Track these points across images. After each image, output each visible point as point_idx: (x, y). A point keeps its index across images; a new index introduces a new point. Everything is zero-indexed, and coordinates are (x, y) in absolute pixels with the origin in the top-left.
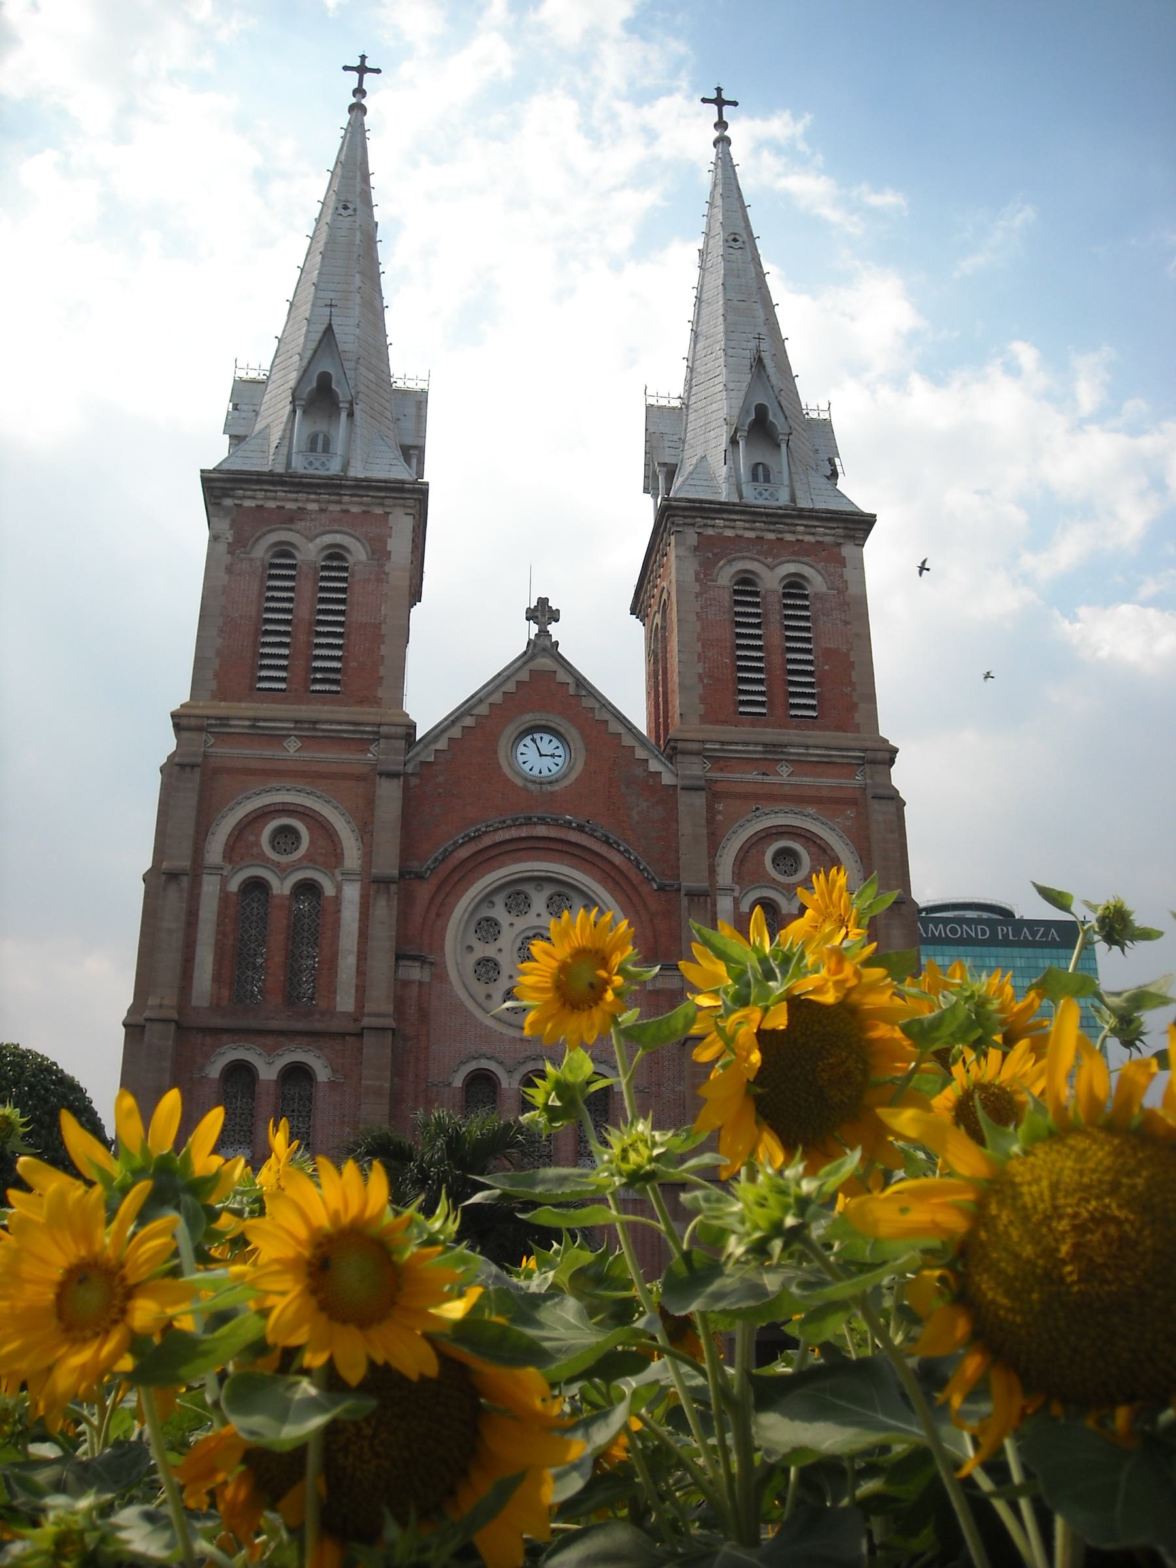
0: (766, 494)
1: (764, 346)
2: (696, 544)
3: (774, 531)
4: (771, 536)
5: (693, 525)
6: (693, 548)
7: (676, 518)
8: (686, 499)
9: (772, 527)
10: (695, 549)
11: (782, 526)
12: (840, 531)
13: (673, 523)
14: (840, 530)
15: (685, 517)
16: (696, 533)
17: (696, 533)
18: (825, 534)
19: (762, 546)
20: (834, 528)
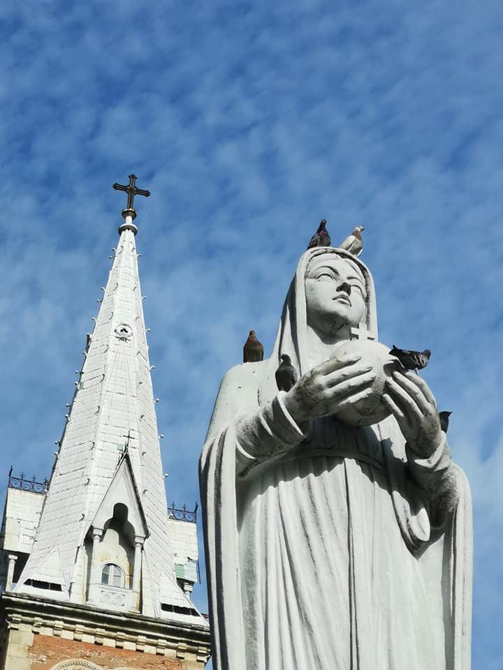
0: (113, 598)
1: (132, 443)
2: (31, 645)
3: (115, 638)
4: (111, 643)
5: (32, 623)
6: (28, 648)
7: (14, 615)
8: (28, 596)
9: (113, 634)
10: (29, 649)
11: (124, 634)
12: (183, 646)
13: (10, 620)
14: (184, 644)
15: (24, 614)
16: (33, 632)
17: (33, 632)
18: (168, 647)
19: (100, 654)
20: (177, 641)
